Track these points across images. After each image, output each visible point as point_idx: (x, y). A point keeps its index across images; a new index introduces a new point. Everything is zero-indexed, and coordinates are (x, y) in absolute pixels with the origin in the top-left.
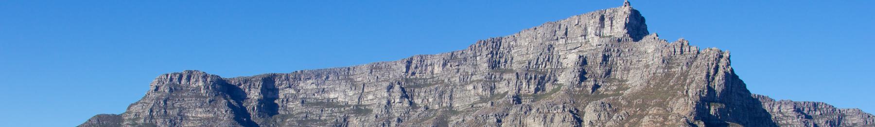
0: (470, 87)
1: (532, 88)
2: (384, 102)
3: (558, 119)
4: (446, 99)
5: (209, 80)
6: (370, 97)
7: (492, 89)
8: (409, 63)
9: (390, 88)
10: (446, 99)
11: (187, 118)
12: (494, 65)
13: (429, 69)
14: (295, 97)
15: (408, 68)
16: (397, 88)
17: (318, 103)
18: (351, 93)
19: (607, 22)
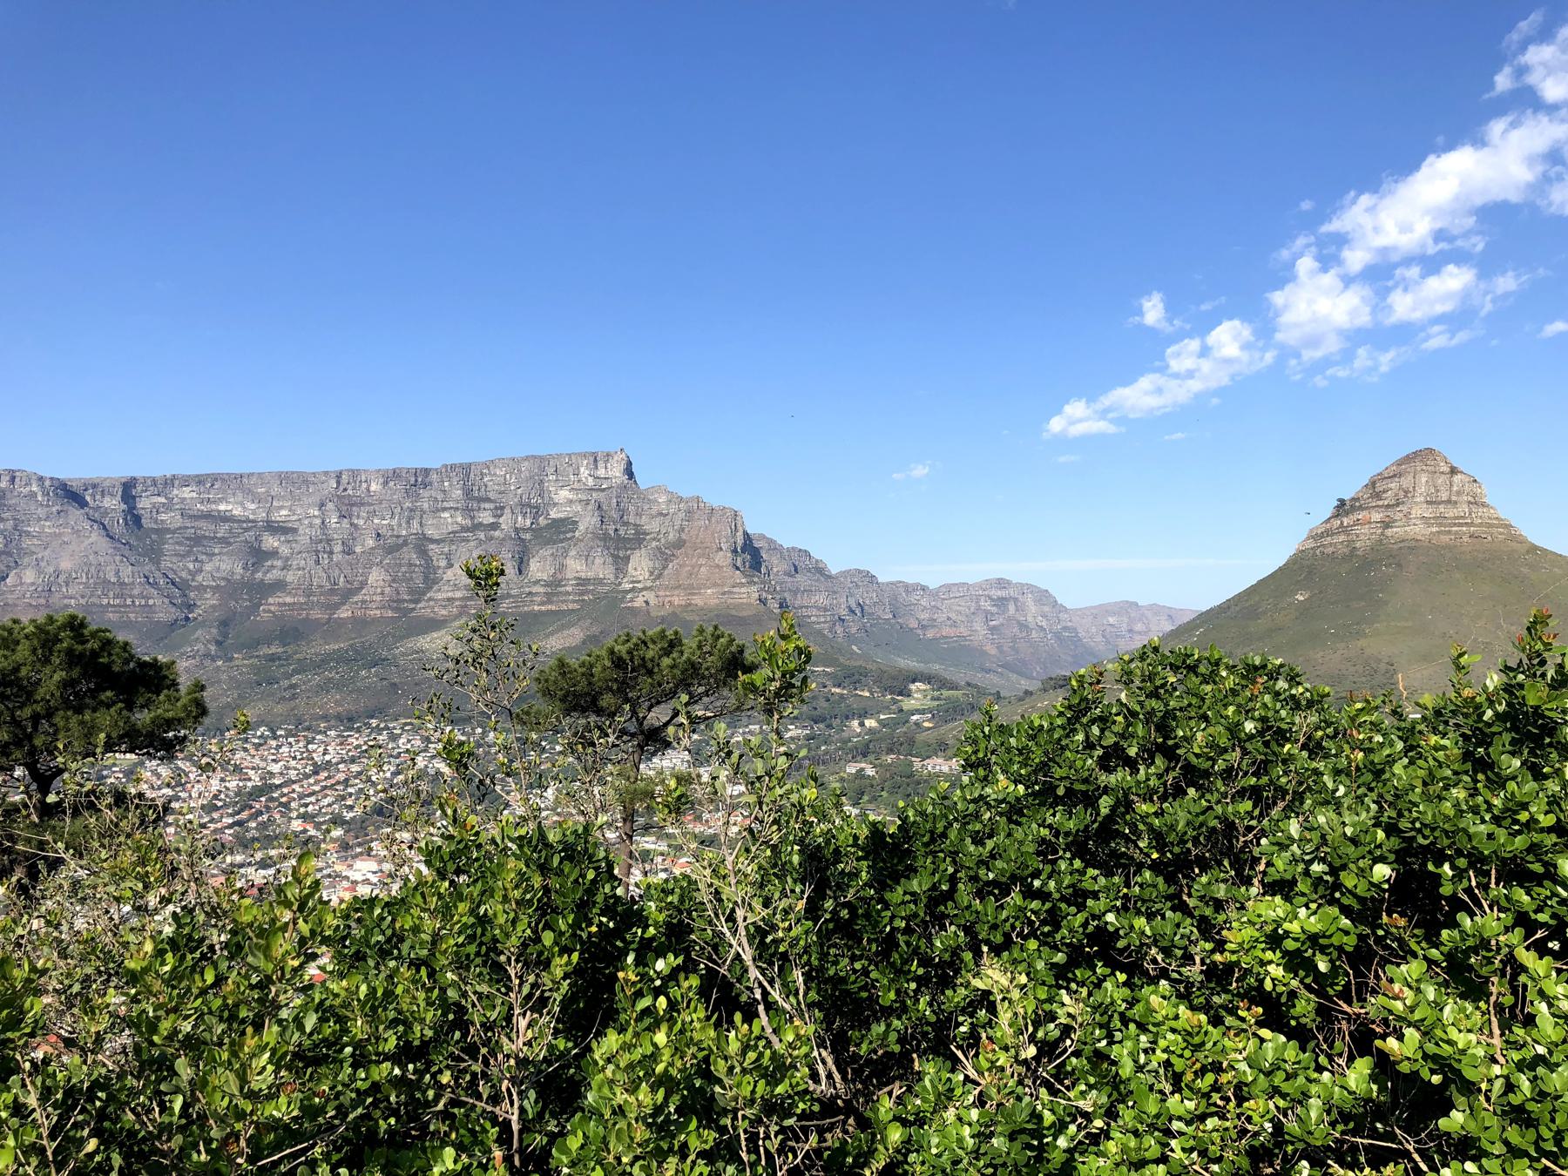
0: (446, 515)
1: (528, 523)
2: (318, 521)
3: (597, 561)
4: (415, 524)
5: (47, 483)
6: (284, 512)
7: (472, 518)
8: (339, 477)
9: (322, 505)
10: (415, 524)
11: (28, 534)
12: (468, 493)
13: (364, 485)
14: (168, 507)
15: (338, 483)
16: (330, 506)
17: (208, 516)
18: (253, 506)
19: (601, 464)
